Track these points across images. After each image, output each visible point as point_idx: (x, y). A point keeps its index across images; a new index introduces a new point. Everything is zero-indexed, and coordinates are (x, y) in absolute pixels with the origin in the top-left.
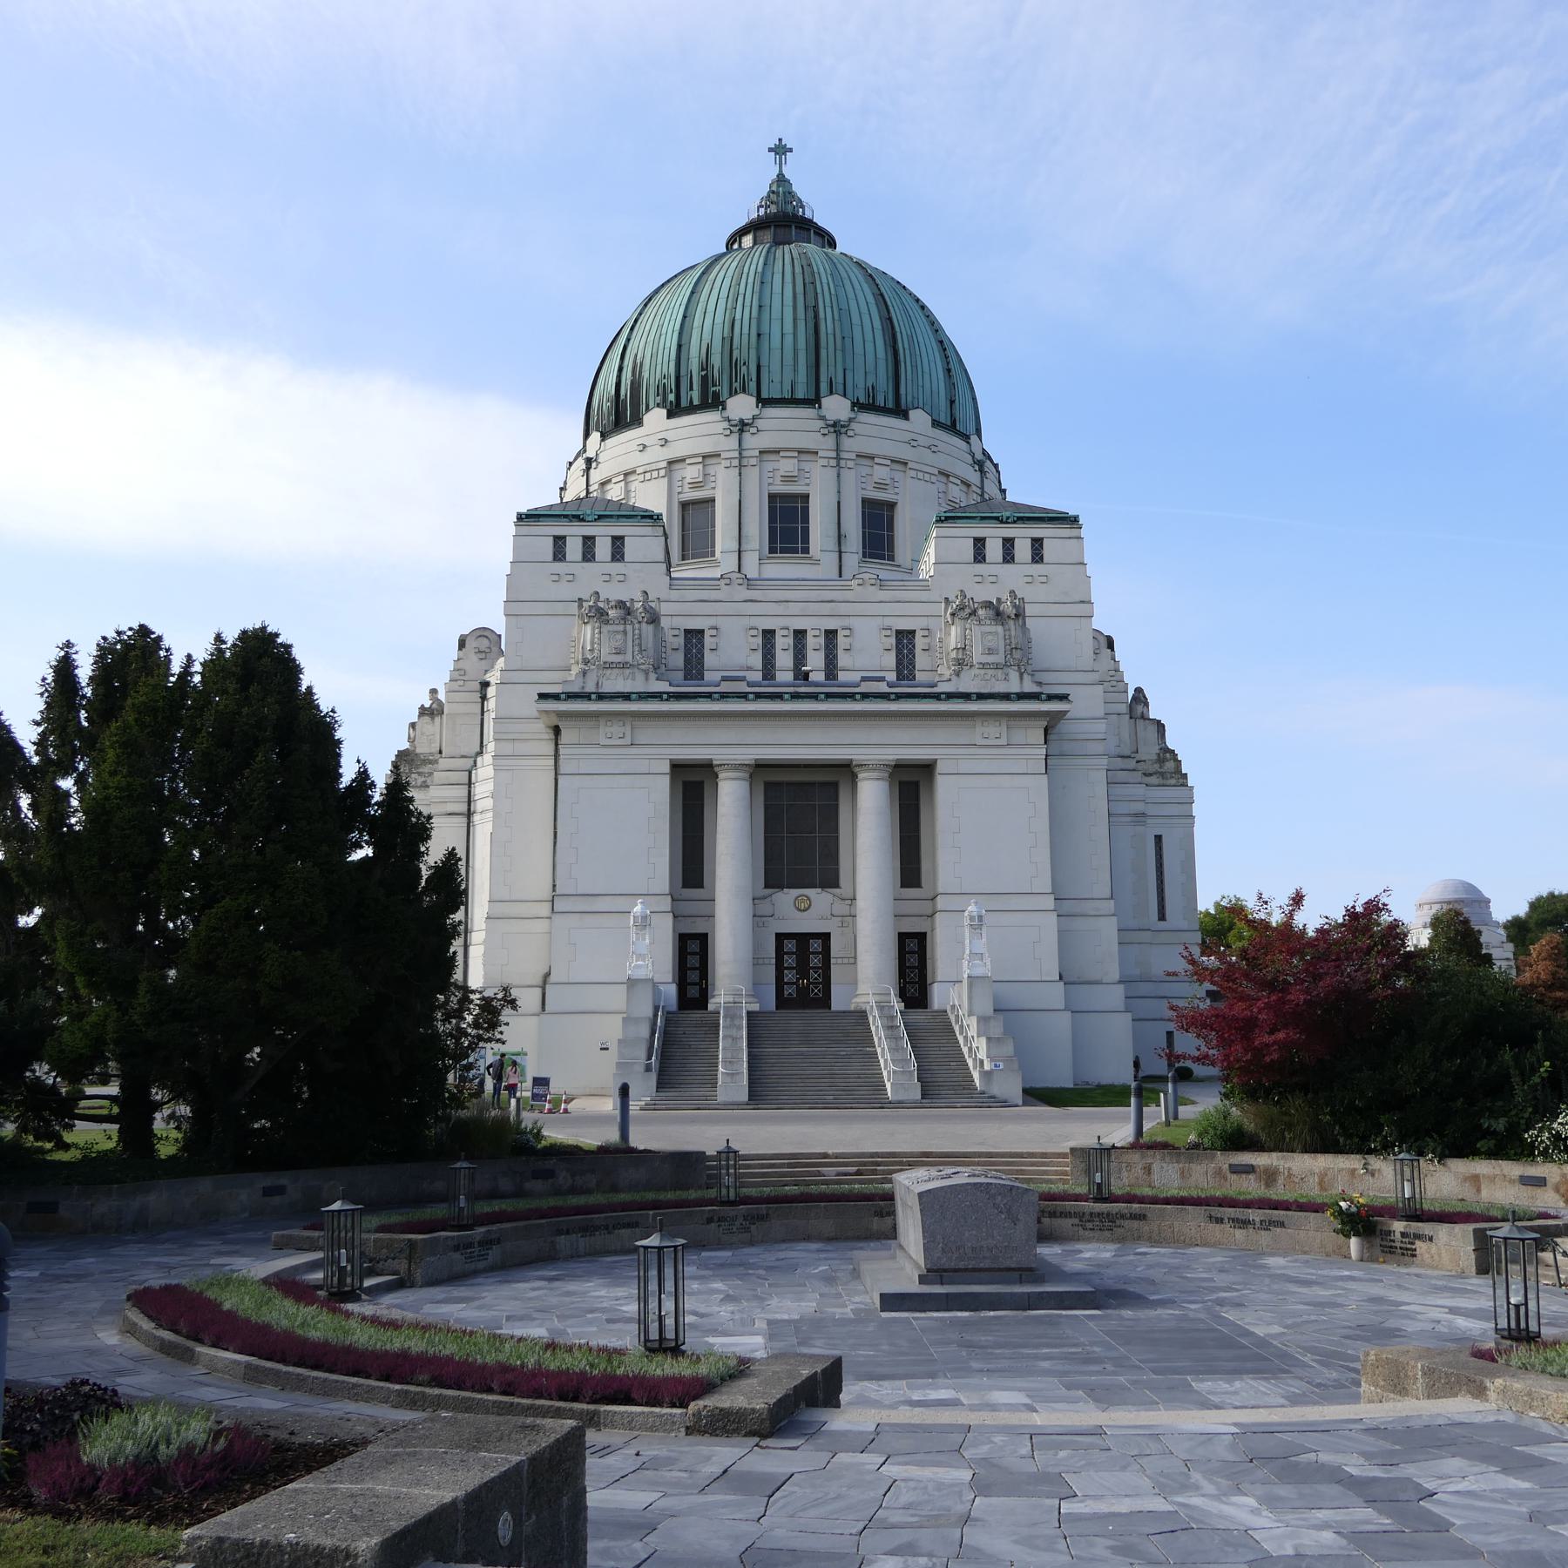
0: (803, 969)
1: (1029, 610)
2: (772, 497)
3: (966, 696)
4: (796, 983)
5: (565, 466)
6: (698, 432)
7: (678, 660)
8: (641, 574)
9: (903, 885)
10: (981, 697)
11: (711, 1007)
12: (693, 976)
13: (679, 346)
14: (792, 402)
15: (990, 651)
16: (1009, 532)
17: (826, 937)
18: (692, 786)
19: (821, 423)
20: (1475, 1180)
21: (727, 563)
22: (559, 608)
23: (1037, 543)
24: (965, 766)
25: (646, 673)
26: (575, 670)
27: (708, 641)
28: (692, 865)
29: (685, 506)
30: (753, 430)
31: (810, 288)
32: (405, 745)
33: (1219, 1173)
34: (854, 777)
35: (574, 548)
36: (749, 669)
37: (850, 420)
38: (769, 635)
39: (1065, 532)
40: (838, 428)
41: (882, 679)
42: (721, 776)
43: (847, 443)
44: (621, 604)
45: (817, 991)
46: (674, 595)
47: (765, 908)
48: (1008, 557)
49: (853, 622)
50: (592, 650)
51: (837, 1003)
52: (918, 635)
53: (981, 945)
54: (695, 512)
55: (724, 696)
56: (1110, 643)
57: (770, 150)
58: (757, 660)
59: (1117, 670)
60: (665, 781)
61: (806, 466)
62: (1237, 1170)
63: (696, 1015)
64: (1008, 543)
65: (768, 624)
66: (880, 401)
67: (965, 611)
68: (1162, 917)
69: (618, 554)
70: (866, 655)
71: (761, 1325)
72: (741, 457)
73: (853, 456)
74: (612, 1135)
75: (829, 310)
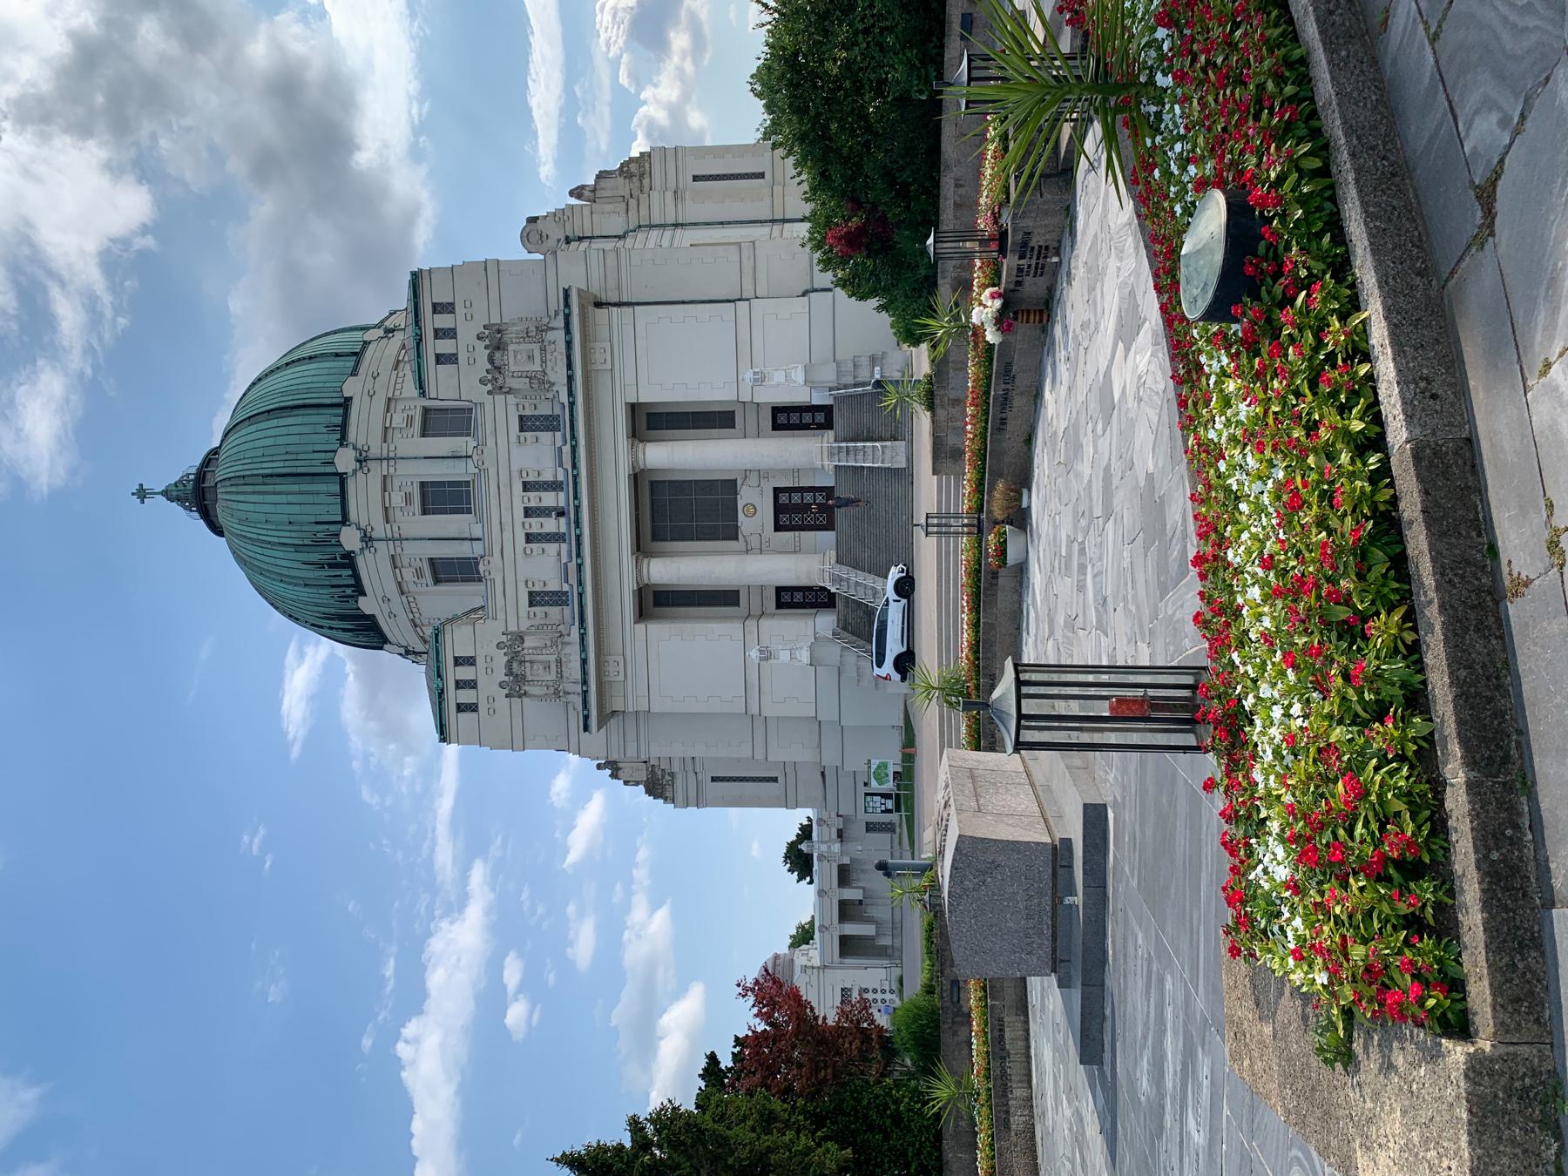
1: (495, 320)
3: (570, 379)
7: (554, 611)
10: (570, 366)
15: (531, 357)
16: (430, 334)
17: (777, 491)
18: (657, 602)
19: (359, 474)
23: (437, 308)
27: (537, 589)
28: (723, 598)
29: (437, 581)
31: (247, 480)
32: (641, 787)
35: (466, 696)
37: (355, 448)
39: (426, 283)
40: (362, 461)
41: (560, 449)
43: (375, 451)
44: (509, 665)
46: (501, 616)
47: (754, 542)
48: (450, 333)
56: (532, 220)
58: (552, 548)
61: (396, 487)
64: (439, 334)
65: (521, 538)
66: (338, 420)
67: (496, 378)
68: (761, 175)
69: (470, 661)
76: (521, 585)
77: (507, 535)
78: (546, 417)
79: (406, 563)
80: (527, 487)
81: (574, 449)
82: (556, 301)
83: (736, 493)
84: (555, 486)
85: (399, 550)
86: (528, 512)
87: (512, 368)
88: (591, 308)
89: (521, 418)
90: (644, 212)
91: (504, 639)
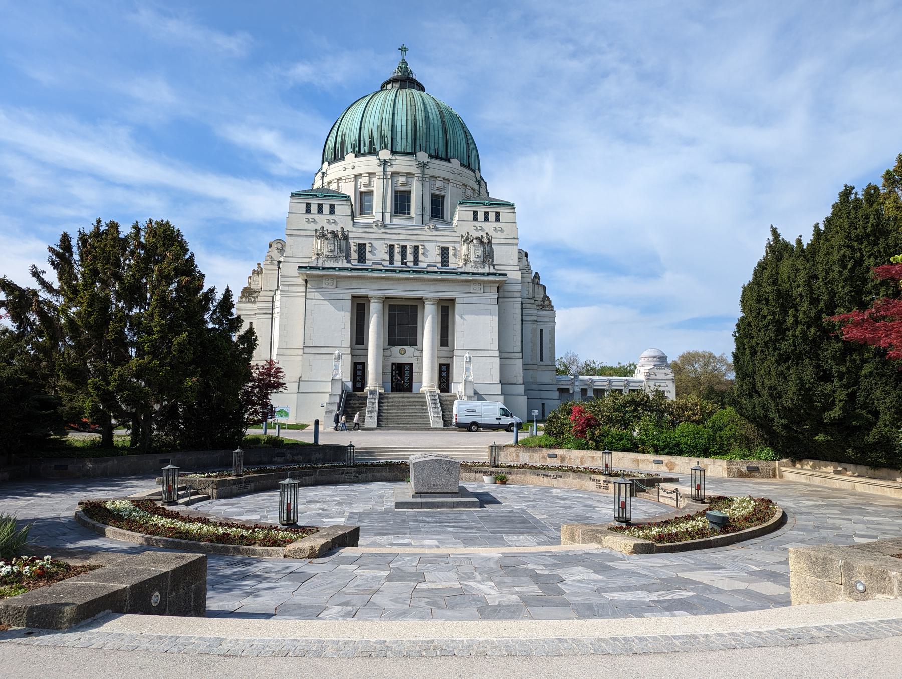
2: (396, 192)
6: (369, 164)
8: (341, 220)
10: (473, 274)
17: (411, 365)
20: (638, 461)
21: (379, 218)
22: (308, 233)
24: (466, 301)
26: (314, 257)
29: (361, 193)
32: (247, 285)
33: (544, 457)
34: (424, 303)
36: (384, 260)
38: (392, 247)
43: (426, 171)
44: (333, 232)
46: (355, 229)
47: (388, 353)
48: (486, 219)
54: (365, 197)
56: (526, 255)
58: (387, 257)
61: (410, 180)
62: (550, 456)
63: (359, 394)
64: (486, 214)
68: (542, 360)
70: (431, 257)
71: (347, 514)
74: (310, 440)
80: (416, 248)
81: (436, 272)
84: (416, 261)
90: (528, 306)
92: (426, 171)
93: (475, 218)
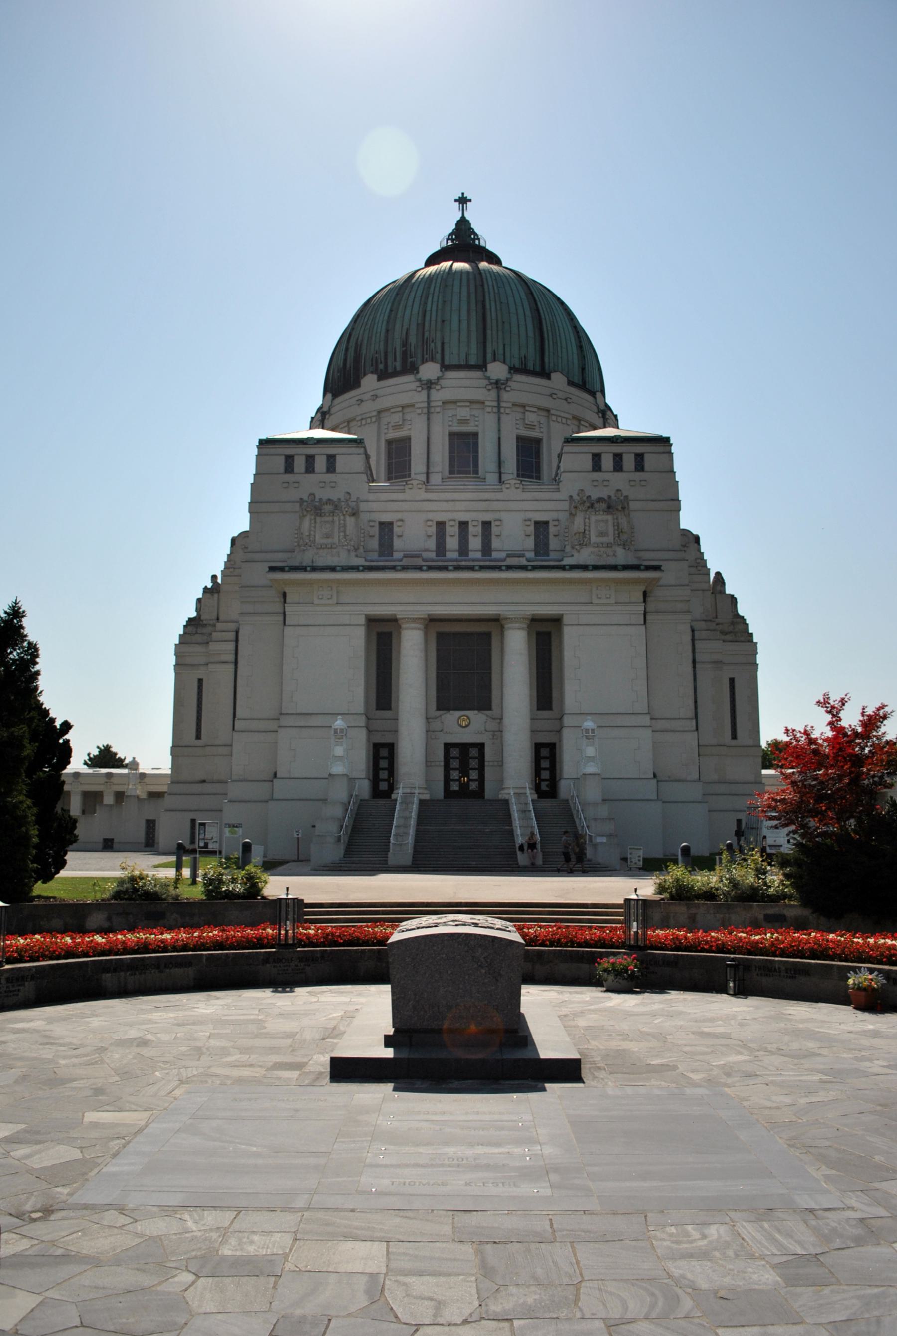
0: (464, 771)
1: (633, 505)
3: (584, 567)
4: (459, 780)
5: (310, 419)
6: (401, 390)
7: (375, 544)
9: (538, 709)
11: (393, 796)
12: (384, 775)
13: (387, 331)
14: (468, 367)
15: (602, 534)
17: (481, 747)
19: (486, 382)
23: (640, 458)
25: (349, 551)
27: (396, 529)
30: (438, 387)
32: (193, 614)
34: (502, 627)
37: (507, 380)
39: (661, 449)
40: (498, 385)
41: (523, 556)
42: (404, 626)
43: (505, 396)
44: (329, 501)
45: (474, 786)
47: (436, 725)
49: (504, 516)
50: (309, 535)
51: (489, 794)
52: (551, 524)
53: (590, 751)
55: (405, 568)
56: (697, 539)
57: (456, 201)
58: (432, 544)
59: (702, 558)
60: (361, 632)
61: (475, 412)
63: (382, 802)
64: (618, 458)
65: (440, 517)
68: (734, 736)
72: (429, 407)
73: (510, 405)
75: (493, 304)
76: (399, 516)
77: (444, 506)
78: (547, 545)
79: (408, 416)
80: (486, 525)
82: (649, 558)
83: (480, 709)
84: (487, 548)
85: (419, 411)
86: (464, 525)
87: (593, 518)
88: (643, 588)
89: (546, 523)
91: (354, 498)
92: (505, 396)
93: (597, 466)
